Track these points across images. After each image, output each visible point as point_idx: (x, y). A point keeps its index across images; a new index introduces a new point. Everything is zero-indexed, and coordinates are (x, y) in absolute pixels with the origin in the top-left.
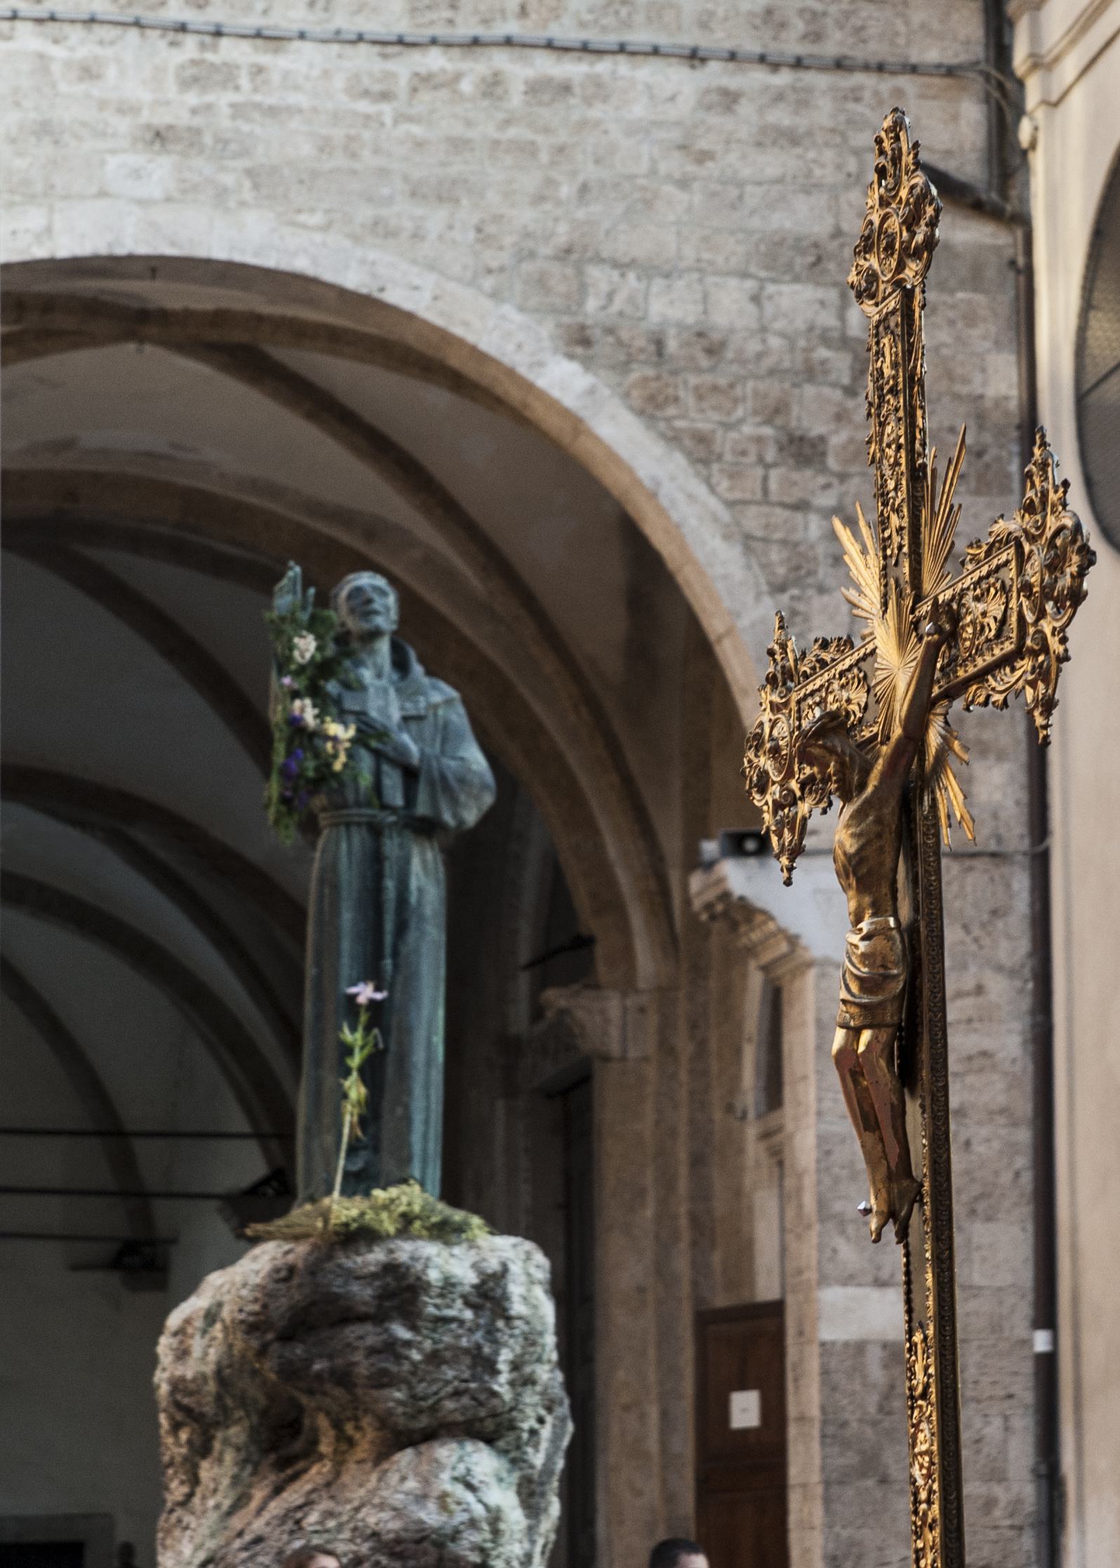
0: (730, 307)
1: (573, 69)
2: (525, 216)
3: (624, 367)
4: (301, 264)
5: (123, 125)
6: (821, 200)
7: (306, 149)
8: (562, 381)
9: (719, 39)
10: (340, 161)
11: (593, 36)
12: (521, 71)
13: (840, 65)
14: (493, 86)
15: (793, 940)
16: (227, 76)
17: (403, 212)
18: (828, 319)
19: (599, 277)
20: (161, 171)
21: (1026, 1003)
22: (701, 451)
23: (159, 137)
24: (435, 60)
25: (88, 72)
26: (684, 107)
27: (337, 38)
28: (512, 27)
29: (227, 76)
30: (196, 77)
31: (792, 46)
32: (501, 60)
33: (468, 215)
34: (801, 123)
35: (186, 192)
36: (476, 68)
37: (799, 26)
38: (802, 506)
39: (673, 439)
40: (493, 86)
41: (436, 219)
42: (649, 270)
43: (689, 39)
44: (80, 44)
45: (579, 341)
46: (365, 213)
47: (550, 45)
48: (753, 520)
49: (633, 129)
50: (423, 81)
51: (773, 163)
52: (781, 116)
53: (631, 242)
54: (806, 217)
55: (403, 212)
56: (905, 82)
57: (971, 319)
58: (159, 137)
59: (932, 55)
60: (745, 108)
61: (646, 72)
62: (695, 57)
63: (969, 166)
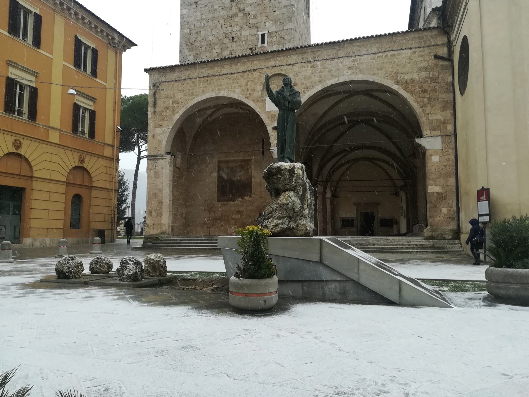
0: (416, 77)
1: (396, 53)
2: (390, 70)
3: (402, 85)
4: (365, 79)
5: (346, 67)
6: (426, 62)
7: (365, 66)
8: (395, 87)
9: (414, 46)
10: (369, 67)
11: (398, 49)
12: (389, 54)
13: (428, 46)
14: (387, 56)
15: (424, 147)
16: (357, 60)
17: (377, 71)
18: (427, 76)
19: (399, 75)
20: (350, 72)
21: (454, 152)
22: (412, 93)
23: (350, 68)
24: (380, 54)
25: (342, 63)
26: (409, 54)
27: (369, 54)
28: (389, 49)
29: (357, 60)
30: (354, 61)
31: (422, 45)
32: (387, 53)
33: (384, 71)
34: (424, 53)
35: (353, 73)
36: (385, 54)
37: (423, 43)
38: (424, 98)
39: (408, 92)
40: (387, 56)
41: (380, 72)
42: (405, 74)
43: (410, 46)
44: (341, 60)
45: (397, 83)
46: (372, 72)
47: (393, 50)
48: (418, 100)
49: (403, 58)
50: (379, 57)
51: (420, 59)
52: (421, 53)
53: (403, 71)
54: (425, 64)
55: (377, 71)
56: (437, 47)
57: (446, 73)
58: (350, 68)
59: (440, 43)
60: (417, 53)
61: (405, 51)
62: (410, 49)
63: (446, 55)
